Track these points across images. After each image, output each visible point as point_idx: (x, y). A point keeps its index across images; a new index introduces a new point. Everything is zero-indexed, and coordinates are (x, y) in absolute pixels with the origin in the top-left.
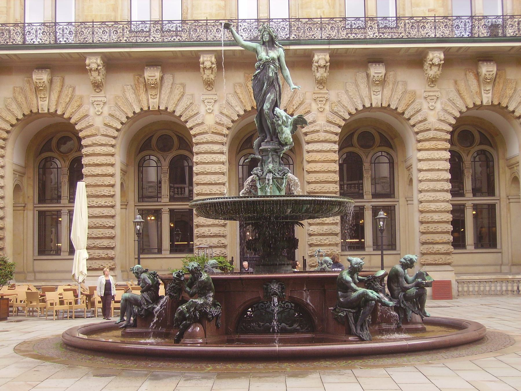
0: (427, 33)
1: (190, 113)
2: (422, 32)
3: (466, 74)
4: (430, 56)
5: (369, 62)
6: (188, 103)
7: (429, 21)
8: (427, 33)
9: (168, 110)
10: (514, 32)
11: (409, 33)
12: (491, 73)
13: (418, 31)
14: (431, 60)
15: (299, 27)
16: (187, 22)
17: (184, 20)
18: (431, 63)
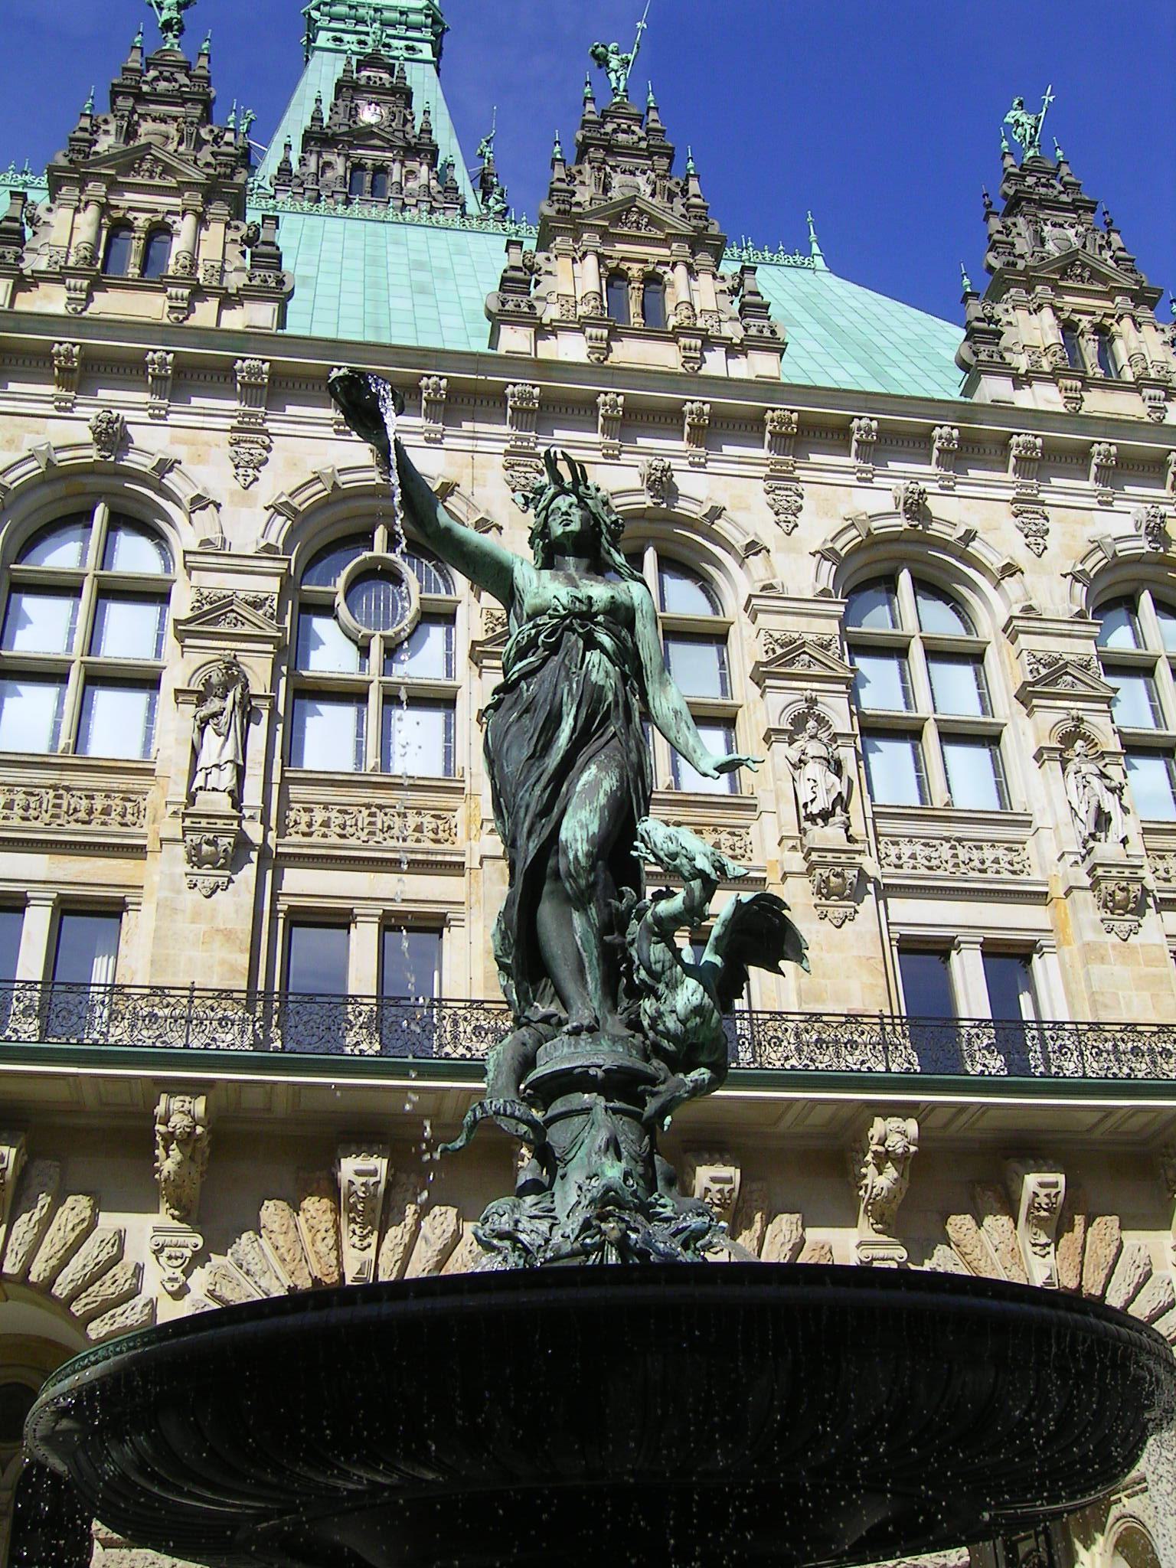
0: (863, 1062)
1: (105, 1289)
2: (849, 1058)
3: (973, 1198)
4: (879, 1127)
5: (686, 1151)
6: (104, 1257)
7: (867, 1028)
8: (863, 1062)
9: (33, 1278)
10: (1108, 1068)
11: (812, 1060)
12: (1054, 1191)
13: (838, 1055)
14: (882, 1142)
15: (481, 1026)
16: (127, 990)
17: (117, 986)
18: (880, 1149)
